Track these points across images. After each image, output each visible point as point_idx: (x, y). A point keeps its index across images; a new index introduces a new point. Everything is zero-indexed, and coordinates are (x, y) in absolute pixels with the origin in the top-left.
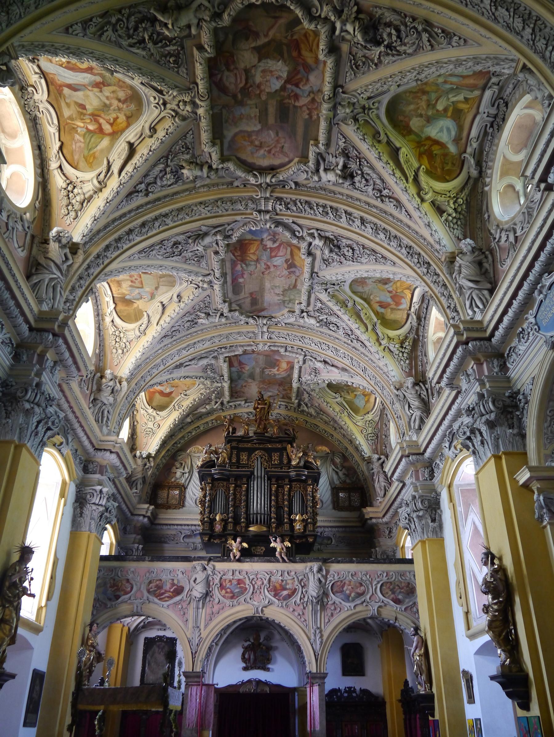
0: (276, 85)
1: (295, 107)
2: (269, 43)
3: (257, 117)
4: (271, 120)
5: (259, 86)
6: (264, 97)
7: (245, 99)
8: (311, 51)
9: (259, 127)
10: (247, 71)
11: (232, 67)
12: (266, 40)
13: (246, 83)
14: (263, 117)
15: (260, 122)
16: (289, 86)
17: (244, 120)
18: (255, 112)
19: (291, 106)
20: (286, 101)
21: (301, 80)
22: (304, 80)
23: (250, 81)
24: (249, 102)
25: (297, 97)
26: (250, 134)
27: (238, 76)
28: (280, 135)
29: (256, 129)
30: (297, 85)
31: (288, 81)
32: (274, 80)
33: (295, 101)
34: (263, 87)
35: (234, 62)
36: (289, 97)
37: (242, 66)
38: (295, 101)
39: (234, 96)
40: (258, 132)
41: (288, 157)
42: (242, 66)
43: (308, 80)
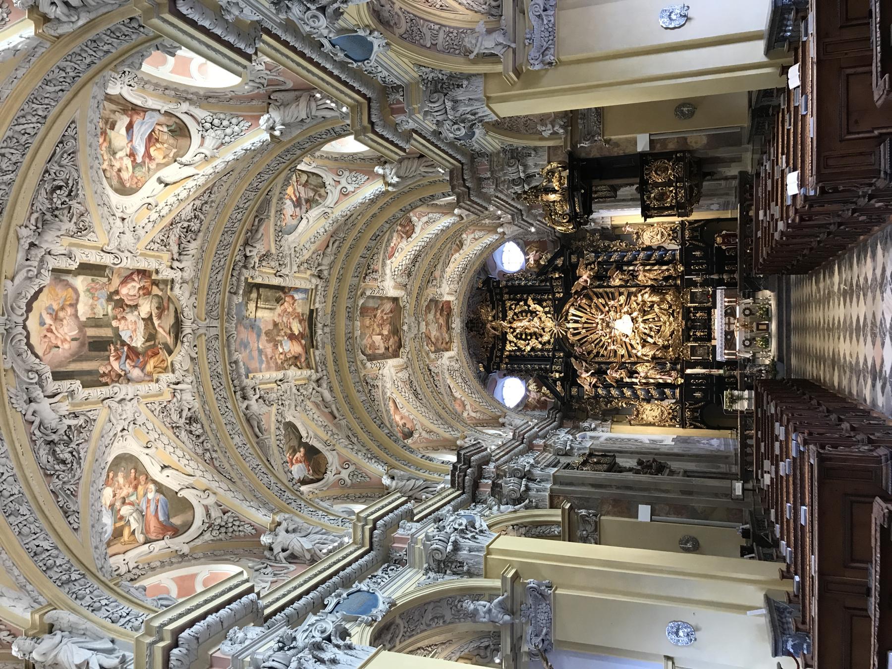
0: (125, 337)
1: (109, 357)
2: (154, 328)
3: (93, 316)
4: (91, 332)
5: (124, 318)
6: (114, 323)
7: (113, 303)
8: (155, 367)
9: (83, 318)
10: (136, 307)
11: (141, 292)
12: (156, 325)
13: (127, 305)
14: (95, 323)
15: (88, 319)
16: (126, 348)
17: (91, 301)
18: (100, 313)
19: (107, 353)
20: (112, 348)
21: (133, 361)
22: (133, 364)
23: (128, 310)
24: (110, 307)
25: (118, 358)
26: (74, 305)
27: (133, 298)
28: (75, 343)
29: (80, 314)
30: (128, 357)
31: (130, 348)
32: (129, 333)
33: (114, 356)
34: (123, 322)
35: (144, 294)
36: (116, 350)
37: (141, 301)
38: (114, 356)
39: (117, 292)
40: (77, 317)
41: (44, 355)
42: (141, 301)
43: (134, 367)
